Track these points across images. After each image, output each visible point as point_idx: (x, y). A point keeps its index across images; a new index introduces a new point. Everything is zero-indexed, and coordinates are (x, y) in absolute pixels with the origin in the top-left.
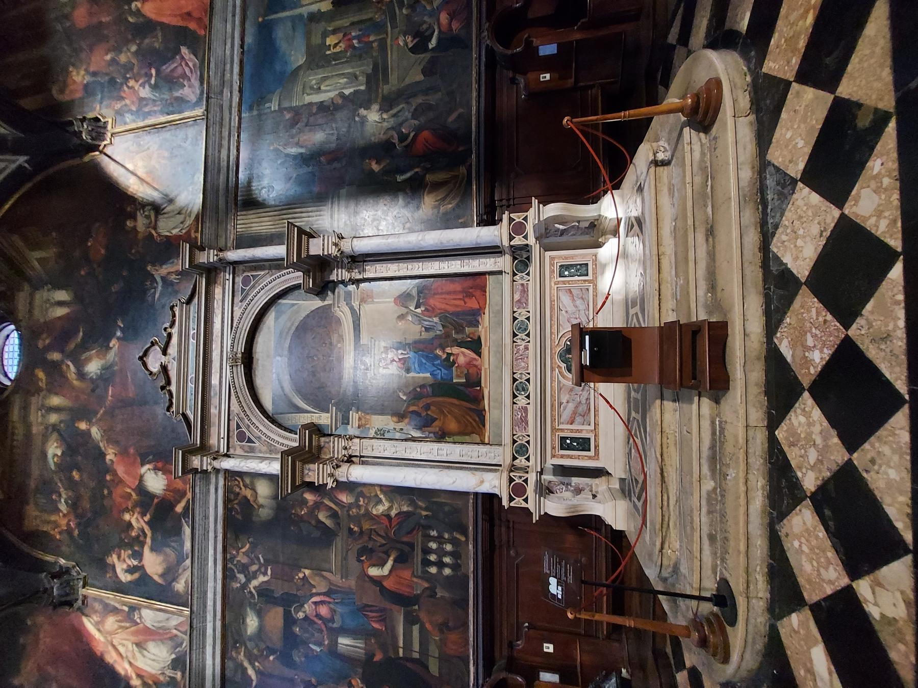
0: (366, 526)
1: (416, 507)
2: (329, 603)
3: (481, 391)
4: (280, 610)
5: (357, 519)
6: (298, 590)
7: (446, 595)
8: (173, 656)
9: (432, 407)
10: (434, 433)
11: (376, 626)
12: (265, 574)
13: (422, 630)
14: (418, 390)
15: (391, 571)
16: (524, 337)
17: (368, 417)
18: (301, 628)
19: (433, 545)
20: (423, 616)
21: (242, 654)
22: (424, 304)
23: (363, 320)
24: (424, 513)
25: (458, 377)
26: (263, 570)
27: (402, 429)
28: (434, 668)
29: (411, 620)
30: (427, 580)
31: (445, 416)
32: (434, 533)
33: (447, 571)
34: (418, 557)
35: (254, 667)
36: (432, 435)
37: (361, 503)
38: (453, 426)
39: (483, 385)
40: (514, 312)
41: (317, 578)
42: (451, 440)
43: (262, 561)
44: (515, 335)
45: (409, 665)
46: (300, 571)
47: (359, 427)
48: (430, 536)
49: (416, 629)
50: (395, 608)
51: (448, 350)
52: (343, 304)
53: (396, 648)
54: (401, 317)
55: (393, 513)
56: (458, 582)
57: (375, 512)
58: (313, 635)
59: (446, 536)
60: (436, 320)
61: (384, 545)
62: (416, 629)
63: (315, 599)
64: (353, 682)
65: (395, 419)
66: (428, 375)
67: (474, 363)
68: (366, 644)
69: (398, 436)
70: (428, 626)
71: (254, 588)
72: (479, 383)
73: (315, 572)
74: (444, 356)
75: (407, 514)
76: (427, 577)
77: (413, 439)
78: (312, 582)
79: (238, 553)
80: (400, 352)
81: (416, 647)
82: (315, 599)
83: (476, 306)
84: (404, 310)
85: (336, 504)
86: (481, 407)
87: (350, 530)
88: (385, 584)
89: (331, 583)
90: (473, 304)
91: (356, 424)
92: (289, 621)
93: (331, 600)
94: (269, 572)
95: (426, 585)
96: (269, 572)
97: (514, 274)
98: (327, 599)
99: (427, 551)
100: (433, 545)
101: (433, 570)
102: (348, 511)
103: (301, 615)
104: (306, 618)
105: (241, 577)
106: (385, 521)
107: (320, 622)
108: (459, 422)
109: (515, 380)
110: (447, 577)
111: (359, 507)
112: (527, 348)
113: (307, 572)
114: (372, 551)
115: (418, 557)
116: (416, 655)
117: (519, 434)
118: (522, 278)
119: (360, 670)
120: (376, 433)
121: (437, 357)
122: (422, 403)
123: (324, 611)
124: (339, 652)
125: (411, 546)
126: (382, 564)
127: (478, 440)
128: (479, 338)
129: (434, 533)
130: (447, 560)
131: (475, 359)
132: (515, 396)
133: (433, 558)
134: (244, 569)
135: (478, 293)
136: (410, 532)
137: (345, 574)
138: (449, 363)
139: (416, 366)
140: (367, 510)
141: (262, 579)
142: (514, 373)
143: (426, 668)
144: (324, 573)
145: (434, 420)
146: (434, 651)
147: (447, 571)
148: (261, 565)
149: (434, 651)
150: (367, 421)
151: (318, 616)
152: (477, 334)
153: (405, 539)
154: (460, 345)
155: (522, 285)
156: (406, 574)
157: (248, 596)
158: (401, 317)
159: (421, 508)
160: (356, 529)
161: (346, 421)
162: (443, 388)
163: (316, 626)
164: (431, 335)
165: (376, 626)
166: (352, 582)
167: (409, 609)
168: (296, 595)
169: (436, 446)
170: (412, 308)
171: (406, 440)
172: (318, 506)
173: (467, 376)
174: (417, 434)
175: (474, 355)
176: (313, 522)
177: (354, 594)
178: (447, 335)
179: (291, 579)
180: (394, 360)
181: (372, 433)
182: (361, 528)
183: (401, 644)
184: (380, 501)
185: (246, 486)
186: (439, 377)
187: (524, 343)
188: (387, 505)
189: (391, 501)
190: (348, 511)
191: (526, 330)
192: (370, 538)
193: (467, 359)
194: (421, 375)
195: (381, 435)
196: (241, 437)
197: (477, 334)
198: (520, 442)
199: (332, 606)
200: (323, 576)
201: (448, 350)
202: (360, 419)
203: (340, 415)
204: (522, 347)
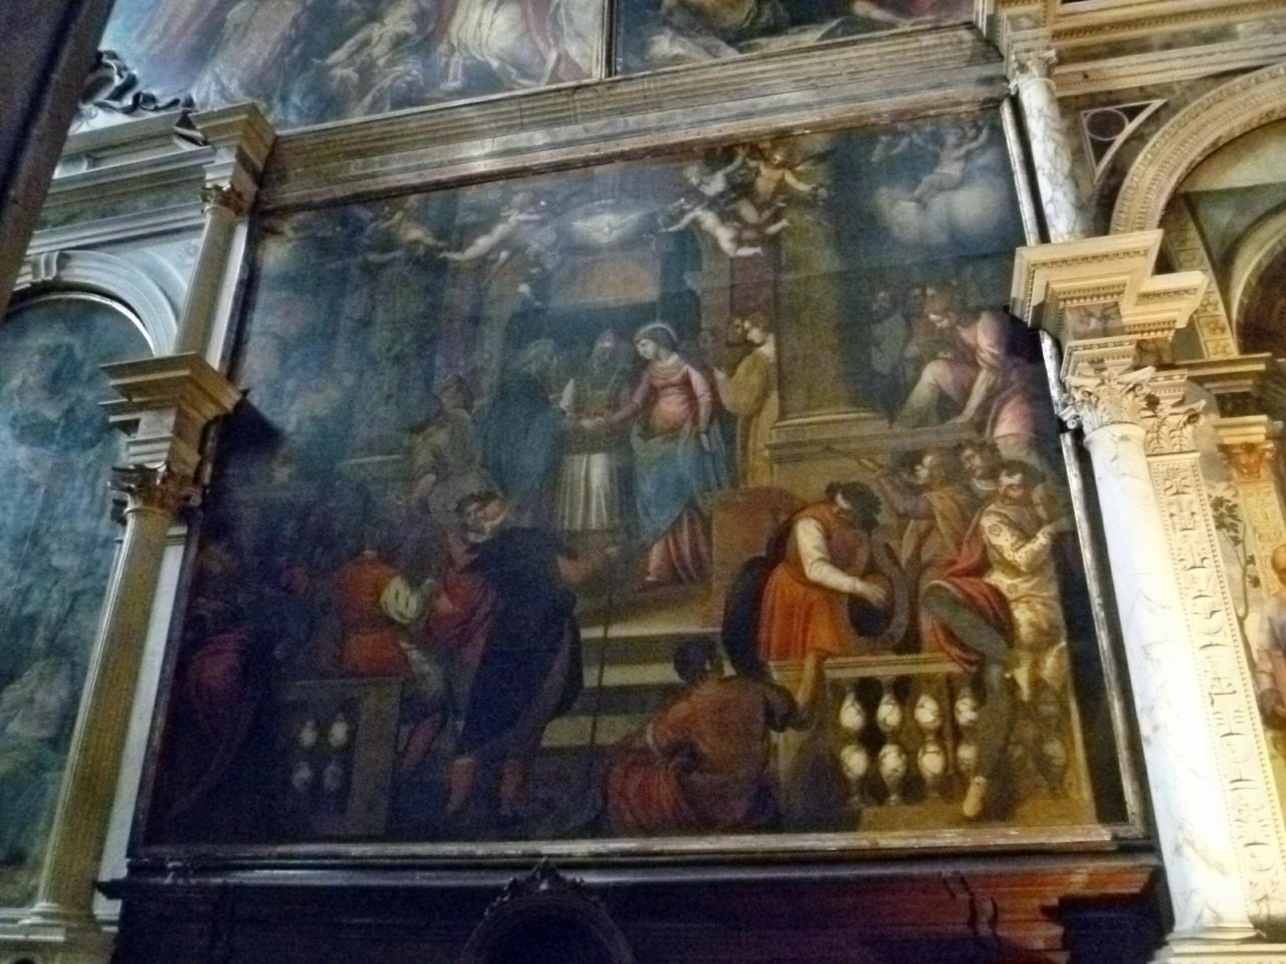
0: (941, 501)
1: (1038, 649)
2: (695, 420)
4: (648, 291)
5: (954, 473)
6: (713, 332)
7: (784, 763)
8: (495, 64)
11: (656, 556)
12: (739, 242)
13: (668, 693)
15: (818, 586)
17: (1265, 472)
18: (614, 352)
19: (927, 712)
20: (708, 692)
21: (523, 217)
24: (1022, 676)
26: (748, 235)
27: (1256, 582)
28: (563, 733)
29: (688, 655)
30: (815, 701)
32: (966, 711)
33: (855, 761)
34: (886, 667)
35: (495, 249)
37: (1005, 480)
41: (755, 379)
43: (773, 229)
45: (560, 663)
46: (766, 330)
47: (1224, 448)
48: (953, 698)
49: (663, 673)
50: (717, 606)
53: (607, 616)
55: (998, 578)
56: (831, 800)
57: (987, 522)
58: (598, 385)
59: (967, 753)
61: (896, 562)
62: (663, 673)
63: (697, 379)
64: (492, 507)
68: (602, 532)
70: (681, 709)
71: (695, 222)
73: (773, 371)
75: (1003, 625)
76: (828, 695)
78: (741, 369)
79: (779, 167)
81: (616, 676)
82: (697, 379)
85: (984, 408)
87: (912, 459)
88: (780, 575)
89: (749, 419)
91: (1233, 437)
92: (629, 321)
93: (702, 425)
94: (746, 251)
95: (801, 697)
96: (746, 251)
98: (704, 412)
99: (904, 691)
100: (927, 712)
101: (851, 716)
102: (970, 443)
103: (647, 348)
104: (642, 364)
105: (716, 184)
106: (967, 559)
107: (638, 399)
110: (837, 765)
111: (992, 474)
113: (768, 350)
114: (869, 524)
115: (886, 667)
116: (590, 678)
119: (526, 521)
123: (671, 406)
124: (567, 459)
125: (911, 643)
126: (838, 557)
129: (966, 711)
130: (891, 759)
133: (888, 713)
134: (742, 189)
136: (951, 636)
137: (790, 453)
140: (990, 498)
141: (724, 236)
143: (563, 708)
144: (774, 397)
146: (612, 730)
147: (855, 761)
148: (759, 228)
149: (612, 730)
150: (1251, 473)
151: (654, 394)
153: (927, 623)
156: (823, 634)
157: (672, 207)
159: (1036, 665)
160: (923, 473)
161: (1232, 405)
163: (625, 392)
165: (656, 556)
166: (764, 476)
167: (721, 651)
168: (696, 329)
172: (966, 358)
176: (912, 350)
177: (734, 483)
179: (739, 309)
181: (1221, 490)
182: (927, 487)
183: (617, 631)
184: (1026, 535)
185: (968, 156)
188: (1021, 557)
189: (1035, 569)
190: (970, 443)
192: (904, 517)
196: (1105, 126)
199: (687, 427)
200: (765, 394)
202: (1250, 448)
203: (1247, 385)
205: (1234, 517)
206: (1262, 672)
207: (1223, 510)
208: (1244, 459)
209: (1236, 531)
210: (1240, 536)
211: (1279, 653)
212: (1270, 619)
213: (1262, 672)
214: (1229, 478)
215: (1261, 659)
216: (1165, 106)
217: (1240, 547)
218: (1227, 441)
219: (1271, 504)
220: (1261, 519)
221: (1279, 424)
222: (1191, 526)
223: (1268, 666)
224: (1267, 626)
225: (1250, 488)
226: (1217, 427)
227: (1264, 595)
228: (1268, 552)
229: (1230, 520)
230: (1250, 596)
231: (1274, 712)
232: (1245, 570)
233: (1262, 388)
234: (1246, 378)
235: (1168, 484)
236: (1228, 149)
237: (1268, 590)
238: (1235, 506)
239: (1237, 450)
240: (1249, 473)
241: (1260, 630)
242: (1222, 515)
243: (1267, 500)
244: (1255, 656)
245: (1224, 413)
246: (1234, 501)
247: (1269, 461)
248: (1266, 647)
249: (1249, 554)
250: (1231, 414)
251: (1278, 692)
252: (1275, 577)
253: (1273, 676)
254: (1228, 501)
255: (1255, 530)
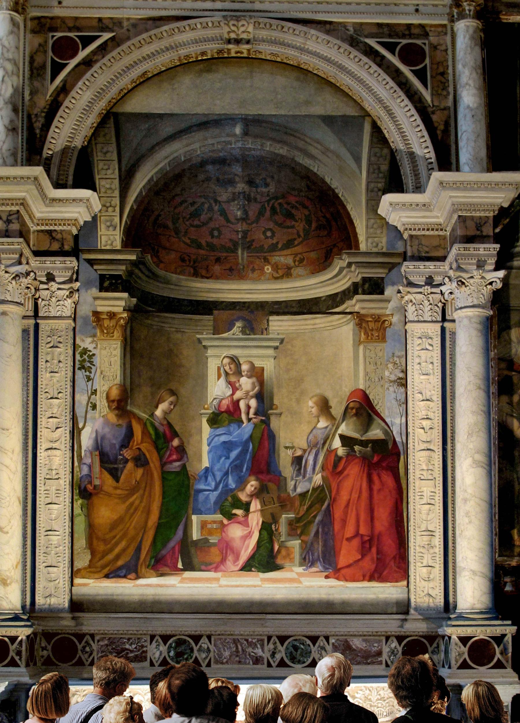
3: (175, 570)
9: (140, 472)
10: (89, 476)
14: (176, 442)
16: (278, 657)
17: (118, 334)
22: (351, 455)
23: (319, 321)
25: (203, 525)
27: (94, 407)
31: (124, 498)
36: (85, 470)
38: (106, 513)
39: (188, 574)
40: (327, 638)
42: (77, 510)
44: (282, 639)
47: (96, 314)
51: (255, 505)
52: (355, 276)
54: (325, 406)
60: (318, 479)
65: (115, 393)
66: (206, 463)
67: (230, 558)
69: (82, 399)
72: (189, 567)
74: (243, 497)
77: (75, 433)
80: (253, 403)
83: (342, 561)
84: (337, 410)
86: (143, 570)
90: (348, 553)
91: (103, 307)
97: (400, 639)
108: (114, 525)
109: (197, 638)
112: (257, 661)
117: (95, 646)
118: (393, 652)
120: (85, 351)
121: (242, 484)
122: (147, 448)
127: (78, 565)
128: (277, 568)
131: (237, 558)
132: (165, 638)
135: (368, 564)
138: (230, 506)
139: (223, 438)
142: (209, 637)
145: (115, 474)
150: (109, 333)
152: (287, 564)
154: (268, 530)
155: (379, 653)
158: (325, 406)
161: (108, 284)
162: (179, 493)
164: (286, 468)
169: (64, 483)
170: (344, 429)
171: (74, 419)
173: (203, 545)
174: (87, 439)
175: (244, 556)
178: (285, 503)
180: (235, 389)
181: (85, 343)
186: (202, 487)
187: (266, 655)
191: (293, 659)
193: (237, 544)
194: (205, 448)
195: (83, 362)
197: (287, 564)
198: (80, 647)
201: (255, 505)
202: (112, 315)
203: (121, 270)
204: (259, 652)
205: (91, 363)
206: (85, 464)
207: (85, 357)
208: (106, 323)
209: (91, 372)
210: (92, 376)
211: (97, 453)
212: (97, 431)
213: (85, 464)
214: (94, 336)
215: (85, 455)
216: (112, 39)
217: (91, 382)
218: (99, 309)
219: (115, 356)
220: (107, 364)
221: (134, 300)
222: (56, 370)
223: (88, 461)
224: (94, 435)
225: (105, 344)
226: (96, 298)
227: (97, 415)
228: (106, 388)
229: (89, 365)
230: (88, 416)
231: (85, 488)
232: (89, 398)
233: (130, 273)
234: (122, 264)
235: (49, 339)
236: (156, 79)
237: (100, 413)
238: (94, 355)
239: (105, 317)
240: (108, 333)
241: (89, 438)
242: (84, 360)
243: (114, 353)
244: (83, 454)
245: (102, 289)
246: (94, 352)
247: (122, 325)
248: (90, 448)
249: (94, 388)
250: (107, 290)
251: (91, 477)
252: (106, 405)
253: (90, 467)
254: (90, 351)
255: (101, 373)
